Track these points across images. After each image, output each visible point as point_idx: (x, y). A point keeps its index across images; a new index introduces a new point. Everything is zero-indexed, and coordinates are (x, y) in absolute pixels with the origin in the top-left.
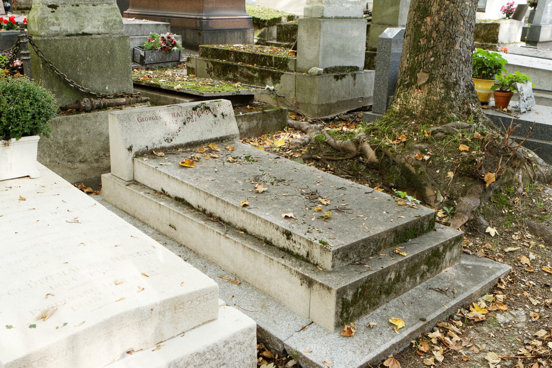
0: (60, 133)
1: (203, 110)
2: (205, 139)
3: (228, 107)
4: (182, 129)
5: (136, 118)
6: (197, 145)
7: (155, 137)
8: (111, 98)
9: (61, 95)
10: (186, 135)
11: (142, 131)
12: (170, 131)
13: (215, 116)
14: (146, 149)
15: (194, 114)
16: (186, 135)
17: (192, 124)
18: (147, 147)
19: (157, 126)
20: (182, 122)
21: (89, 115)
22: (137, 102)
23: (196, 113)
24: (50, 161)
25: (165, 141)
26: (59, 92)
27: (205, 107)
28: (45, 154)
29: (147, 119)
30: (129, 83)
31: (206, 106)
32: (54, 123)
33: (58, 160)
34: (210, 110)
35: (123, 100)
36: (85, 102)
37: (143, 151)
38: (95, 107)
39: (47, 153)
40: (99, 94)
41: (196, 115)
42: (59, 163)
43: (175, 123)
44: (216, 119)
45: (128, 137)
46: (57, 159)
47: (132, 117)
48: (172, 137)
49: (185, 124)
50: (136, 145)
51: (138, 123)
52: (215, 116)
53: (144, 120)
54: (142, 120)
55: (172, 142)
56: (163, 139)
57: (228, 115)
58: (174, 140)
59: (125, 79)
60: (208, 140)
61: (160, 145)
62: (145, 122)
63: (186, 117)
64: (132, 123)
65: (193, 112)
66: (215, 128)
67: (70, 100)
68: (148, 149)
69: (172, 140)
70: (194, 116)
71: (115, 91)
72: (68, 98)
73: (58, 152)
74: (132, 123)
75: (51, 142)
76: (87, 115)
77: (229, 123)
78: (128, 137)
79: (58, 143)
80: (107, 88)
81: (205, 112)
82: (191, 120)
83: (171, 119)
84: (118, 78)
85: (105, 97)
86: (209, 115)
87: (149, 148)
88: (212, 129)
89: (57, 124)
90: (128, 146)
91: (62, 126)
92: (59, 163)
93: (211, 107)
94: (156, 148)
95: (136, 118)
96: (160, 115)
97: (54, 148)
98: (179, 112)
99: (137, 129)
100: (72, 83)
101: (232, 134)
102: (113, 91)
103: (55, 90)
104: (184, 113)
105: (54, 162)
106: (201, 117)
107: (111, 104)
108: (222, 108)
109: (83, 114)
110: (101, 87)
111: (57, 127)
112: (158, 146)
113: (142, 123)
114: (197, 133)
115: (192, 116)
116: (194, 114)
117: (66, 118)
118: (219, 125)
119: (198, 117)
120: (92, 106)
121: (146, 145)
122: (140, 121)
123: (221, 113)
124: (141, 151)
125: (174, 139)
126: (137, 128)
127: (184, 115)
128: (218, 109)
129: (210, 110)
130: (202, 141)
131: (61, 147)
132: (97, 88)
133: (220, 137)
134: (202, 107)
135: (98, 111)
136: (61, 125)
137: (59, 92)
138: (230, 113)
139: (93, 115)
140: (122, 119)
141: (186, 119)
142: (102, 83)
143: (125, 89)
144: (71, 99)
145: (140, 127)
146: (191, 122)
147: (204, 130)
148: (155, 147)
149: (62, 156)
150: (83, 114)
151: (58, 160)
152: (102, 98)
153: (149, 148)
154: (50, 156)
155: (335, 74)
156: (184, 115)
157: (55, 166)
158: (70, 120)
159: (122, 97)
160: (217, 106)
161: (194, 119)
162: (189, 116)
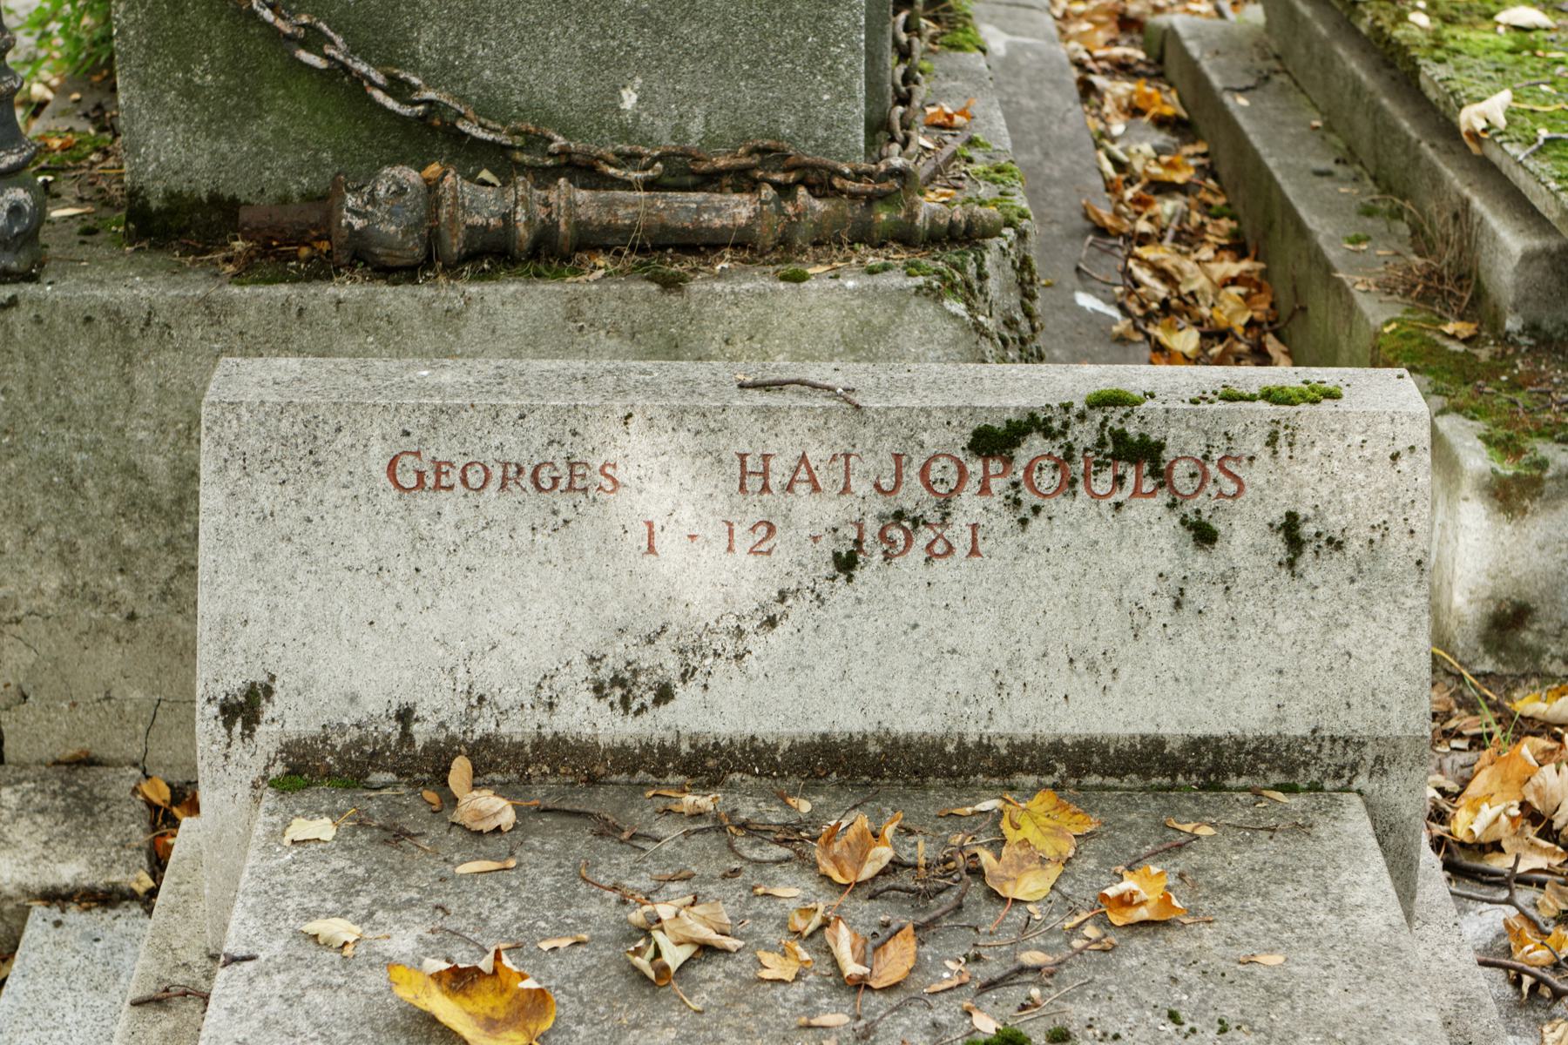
0: (149, 405)
1: (1078, 467)
2: (1025, 734)
3: (1382, 467)
4: (798, 608)
5: (377, 448)
6: (932, 770)
7: (508, 643)
8: (627, 185)
9: (249, 116)
10: (826, 671)
11: (402, 568)
12: (675, 615)
13: (1204, 535)
14: (392, 729)
15: (972, 485)
16: (826, 671)
17: (925, 574)
18: (405, 716)
19: (555, 553)
20: (827, 546)
21: (389, 296)
22: (865, 236)
23: (997, 485)
24: (67, 591)
25: (599, 690)
26: (229, 91)
27: (1120, 437)
28: (31, 532)
29: (474, 479)
30: (831, 73)
31: (1132, 430)
32: (105, 326)
33: (126, 592)
34: (1162, 476)
35: (738, 209)
36: (373, 200)
37: (359, 744)
38: (455, 245)
39: (49, 531)
40: (535, 141)
41: (996, 502)
42: (132, 617)
43: (743, 540)
44: (1200, 561)
45: (257, 607)
46: (122, 587)
47: (345, 438)
48: (673, 667)
49: (846, 564)
50: (309, 682)
51: (389, 499)
52: (1204, 535)
53: (455, 477)
54: (434, 479)
55: (665, 713)
56: (583, 670)
57: (1354, 546)
58: (686, 695)
59: (796, 44)
60: (1057, 748)
61: (541, 716)
62: (452, 504)
63: (879, 505)
64: (332, 496)
65: (975, 466)
66: (1162, 652)
67: (317, 165)
68: (406, 737)
69: (664, 694)
70: (969, 505)
71: (696, 127)
72: (303, 144)
73: (130, 538)
74: (332, 496)
75: (78, 457)
76: (372, 299)
77: (1333, 623)
78: (257, 607)
79: (131, 470)
80: (629, 99)
81: (1103, 483)
82: (924, 536)
83: (722, 502)
84: (728, 30)
85: (586, 172)
86: (1130, 514)
87: (422, 733)
88: (1132, 648)
89: (127, 339)
90: (1256, 462)
91: (167, 356)
92: (132, 617)
93: (1181, 443)
94: (486, 741)
95: (377, 448)
96: (613, 455)
97: (97, 504)
98: (816, 454)
99: (363, 551)
100: (313, 39)
101: (1333, 725)
102: (679, 131)
103: (203, 77)
104: (873, 464)
105: (95, 600)
106: (1037, 524)
107: (608, 229)
108: (1306, 473)
109: (343, 293)
110: (574, 83)
111: (128, 359)
112: (519, 728)
113: (425, 500)
114: (954, 667)
115: (945, 507)
116: (972, 485)
117: (206, 302)
118: (1213, 624)
119: (1007, 520)
120: (433, 241)
121: (402, 697)
122: (410, 480)
123: (1278, 515)
124: (339, 743)
125: (693, 688)
126: (362, 543)
127: (861, 487)
128: (1255, 476)
129: (1162, 476)
130: (984, 748)
131: (155, 507)
132: (546, 91)
133: (1196, 745)
134: (1084, 435)
135: (481, 276)
136: (162, 345)
137: (229, 91)
138: (1385, 528)
139: (428, 306)
140: (253, 443)
141: (872, 527)
142: (592, 57)
143: (787, 124)
144: (326, 156)
145: (388, 535)
146: (917, 554)
147: (1029, 653)
148: (485, 725)
149: (163, 573)
150: (348, 290)
151: (126, 592)
152: (545, 176)
153: (422, 733)
154: (66, 555)
155: (1437, 651)
156: (861, 487)
157: (102, 630)
158: (237, 321)
159: (743, 180)
160: (1255, 444)
161: (958, 531)
162: (913, 496)
